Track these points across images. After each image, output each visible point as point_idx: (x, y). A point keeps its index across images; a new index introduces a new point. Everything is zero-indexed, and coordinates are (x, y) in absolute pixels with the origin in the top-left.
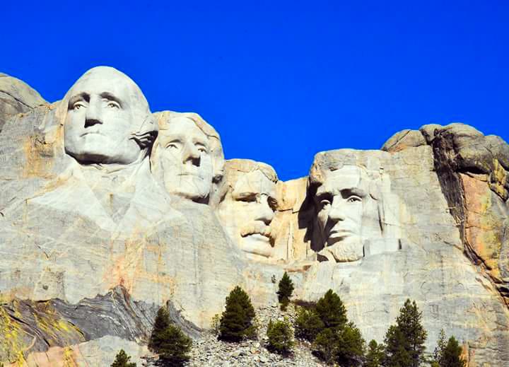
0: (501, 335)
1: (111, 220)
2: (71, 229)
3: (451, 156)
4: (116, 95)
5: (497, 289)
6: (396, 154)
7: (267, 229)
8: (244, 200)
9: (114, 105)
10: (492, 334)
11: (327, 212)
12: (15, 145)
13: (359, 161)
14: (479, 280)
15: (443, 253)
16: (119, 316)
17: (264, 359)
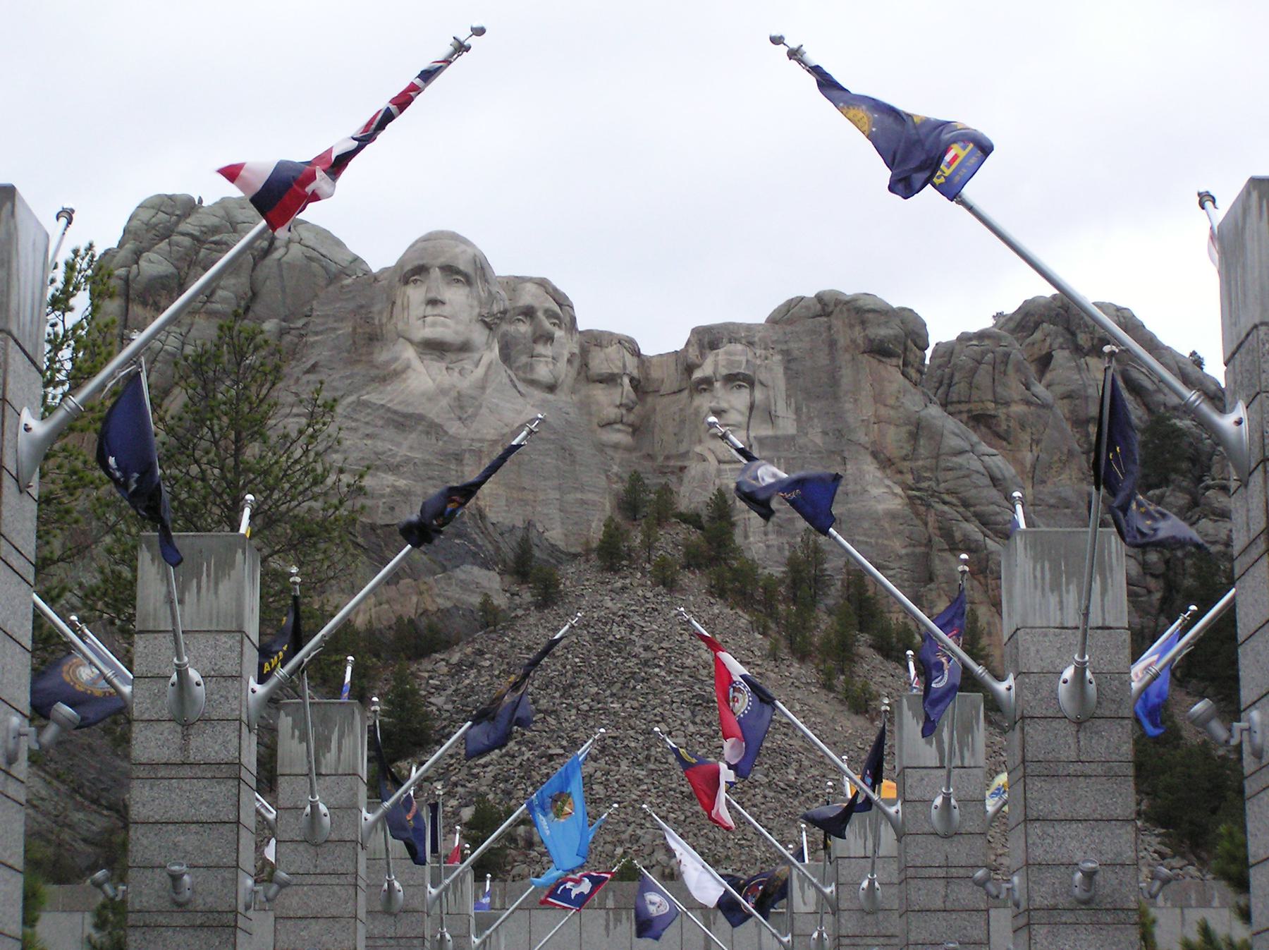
0: (913, 554)
1: (458, 423)
2: (413, 436)
3: (858, 333)
4: (462, 268)
5: (909, 497)
6: (789, 329)
7: (631, 418)
8: (601, 382)
9: (458, 281)
10: (904, 551)
11: (704, 402)
12: (336, 325)
13: (746, 337)
14: (888, 486)
15: (846, 454)
16: (475, 540)
17: (649, 595)
